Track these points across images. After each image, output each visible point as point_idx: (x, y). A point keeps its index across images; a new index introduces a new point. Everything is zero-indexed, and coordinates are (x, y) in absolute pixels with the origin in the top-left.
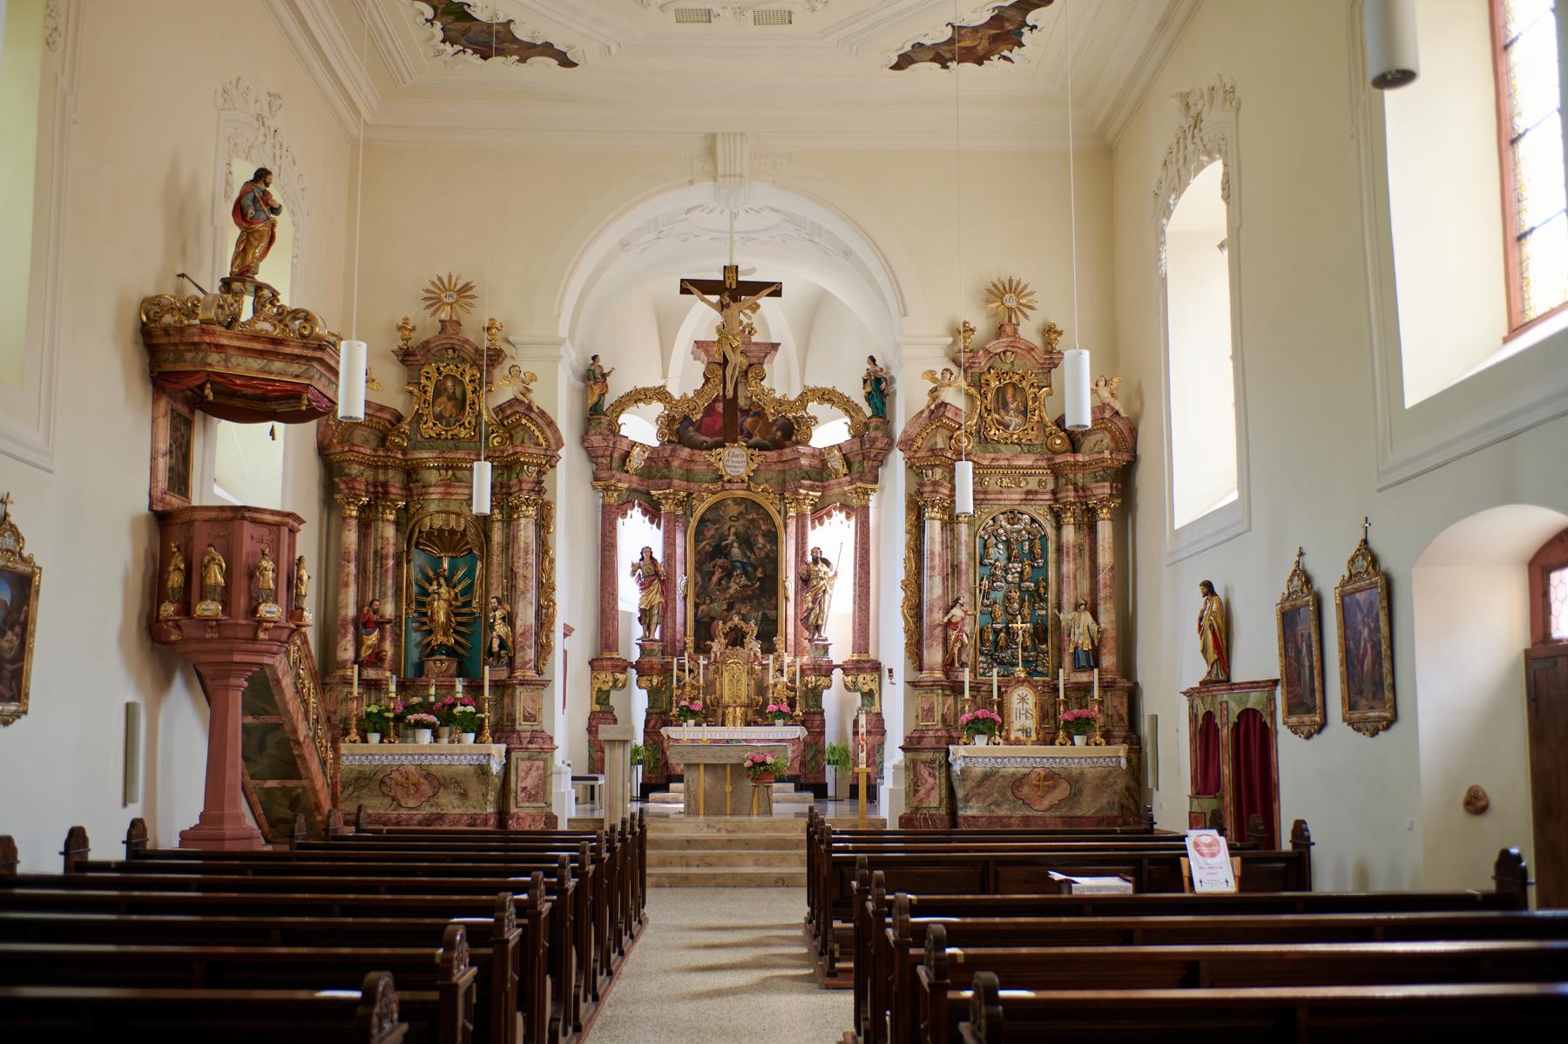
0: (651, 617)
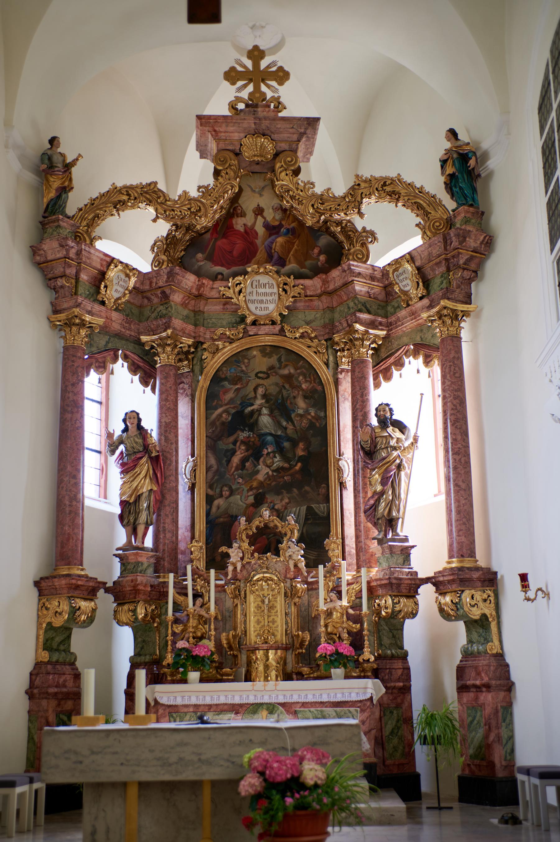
0: (137, 514)
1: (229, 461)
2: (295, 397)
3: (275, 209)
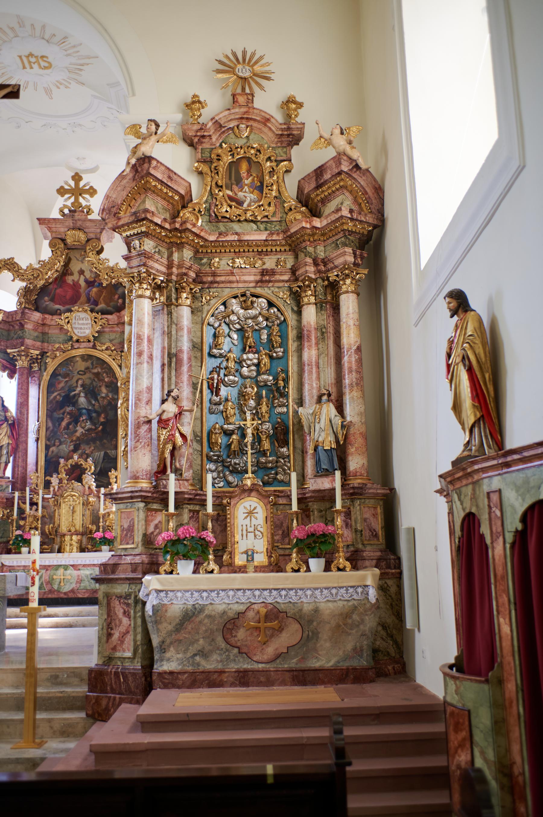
1: (60, 425)
2: (100, 387)
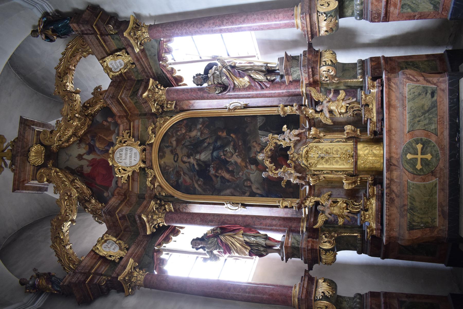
0: (258, 245)
1: (228, 181)
2: (190, 138)
3: (79, 147)
